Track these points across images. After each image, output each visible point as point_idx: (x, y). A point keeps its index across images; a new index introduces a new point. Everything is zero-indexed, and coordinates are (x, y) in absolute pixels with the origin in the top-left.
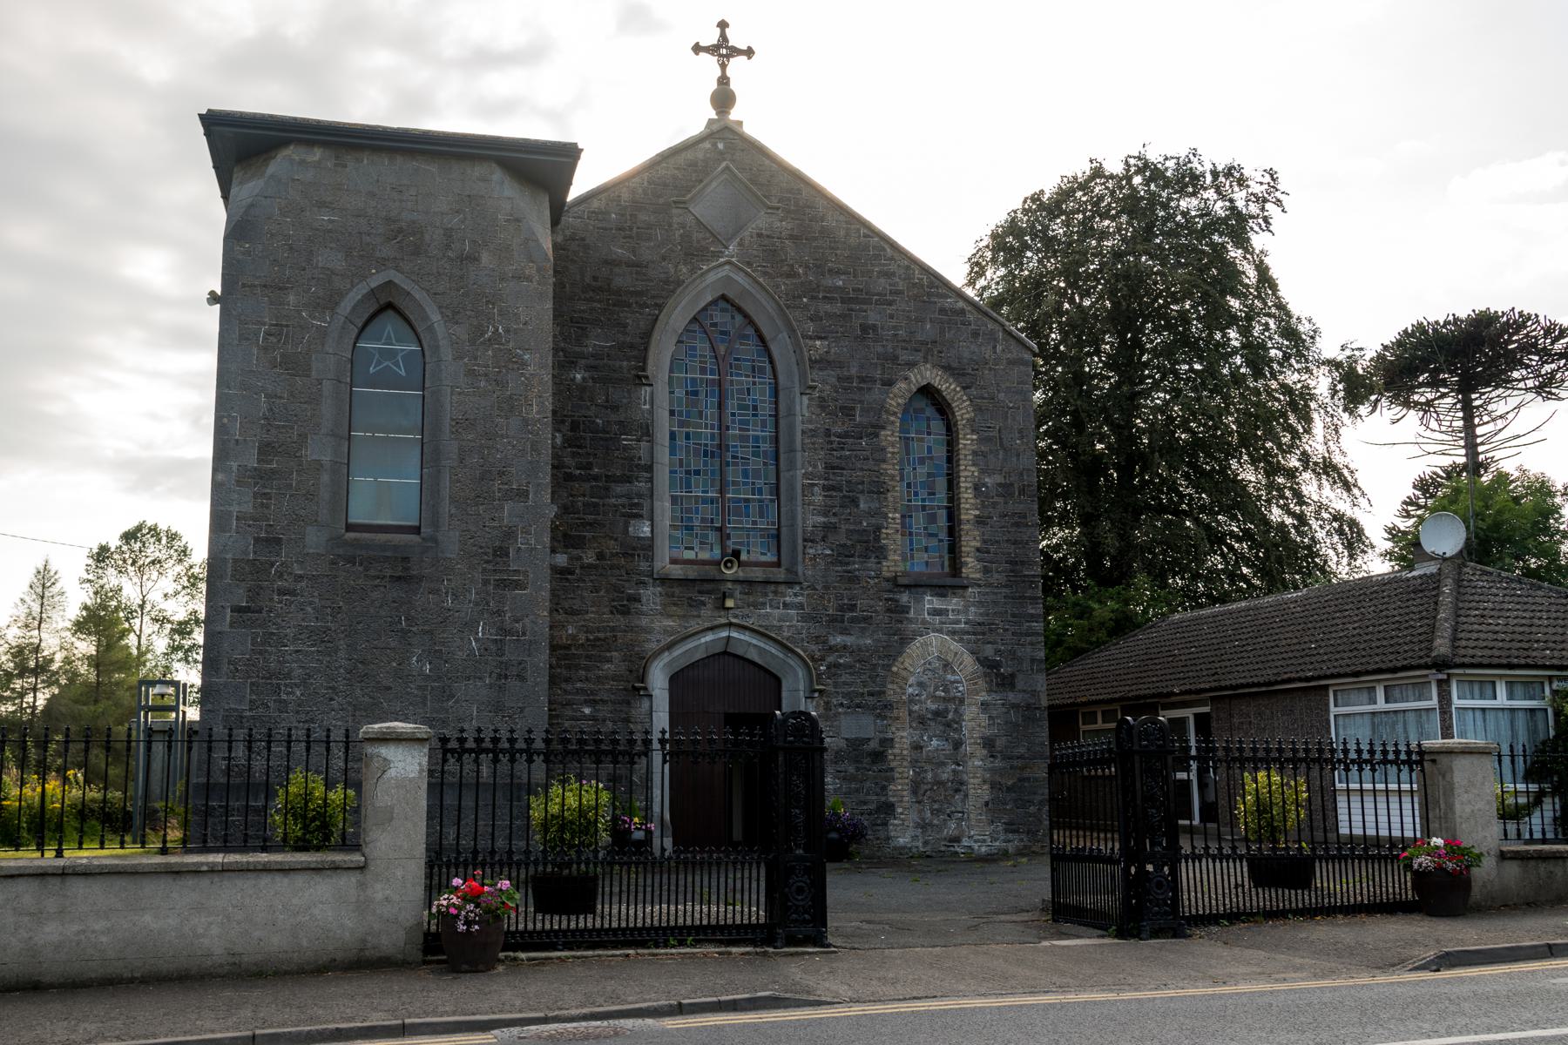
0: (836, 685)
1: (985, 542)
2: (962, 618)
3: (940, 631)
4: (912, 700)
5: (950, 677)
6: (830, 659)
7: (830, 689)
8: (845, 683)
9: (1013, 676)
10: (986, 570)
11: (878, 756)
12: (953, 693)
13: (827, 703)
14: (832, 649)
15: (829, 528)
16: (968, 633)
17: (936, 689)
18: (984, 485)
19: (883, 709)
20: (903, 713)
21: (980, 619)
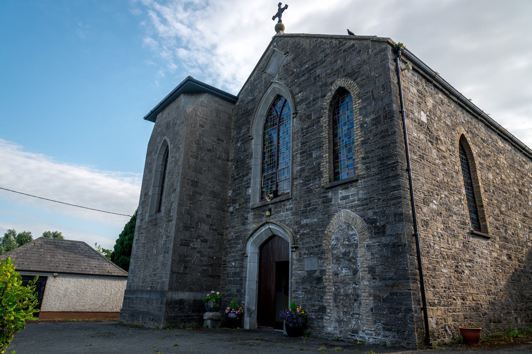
0: (303, 244)
1: (366, 153)
2: (356, 198)
3: (345, 208)
4: (334, 247)
5: (351, 233)
6: (301, 232)
7: (301, 246)
8: (306, 243)
9: (384, 226)
10: (367, 168)
11: (319, 280)
12: (352, 241)
13: (300, 253)
14: (302, 227)
15: (302, 170)
16: (359, 206)
17: (344, 240)
18: (366, 123)
19: (319, 253)
20: (329, 255)
21: (364, 197)
